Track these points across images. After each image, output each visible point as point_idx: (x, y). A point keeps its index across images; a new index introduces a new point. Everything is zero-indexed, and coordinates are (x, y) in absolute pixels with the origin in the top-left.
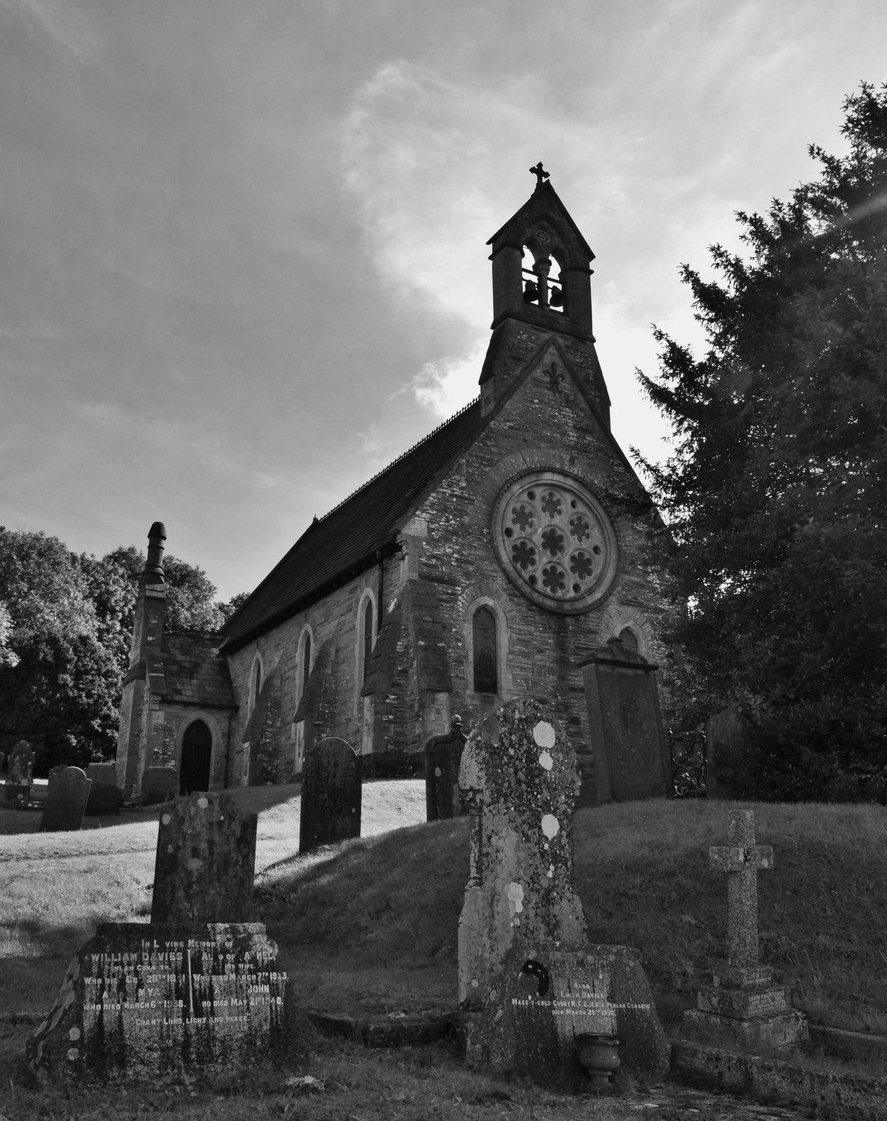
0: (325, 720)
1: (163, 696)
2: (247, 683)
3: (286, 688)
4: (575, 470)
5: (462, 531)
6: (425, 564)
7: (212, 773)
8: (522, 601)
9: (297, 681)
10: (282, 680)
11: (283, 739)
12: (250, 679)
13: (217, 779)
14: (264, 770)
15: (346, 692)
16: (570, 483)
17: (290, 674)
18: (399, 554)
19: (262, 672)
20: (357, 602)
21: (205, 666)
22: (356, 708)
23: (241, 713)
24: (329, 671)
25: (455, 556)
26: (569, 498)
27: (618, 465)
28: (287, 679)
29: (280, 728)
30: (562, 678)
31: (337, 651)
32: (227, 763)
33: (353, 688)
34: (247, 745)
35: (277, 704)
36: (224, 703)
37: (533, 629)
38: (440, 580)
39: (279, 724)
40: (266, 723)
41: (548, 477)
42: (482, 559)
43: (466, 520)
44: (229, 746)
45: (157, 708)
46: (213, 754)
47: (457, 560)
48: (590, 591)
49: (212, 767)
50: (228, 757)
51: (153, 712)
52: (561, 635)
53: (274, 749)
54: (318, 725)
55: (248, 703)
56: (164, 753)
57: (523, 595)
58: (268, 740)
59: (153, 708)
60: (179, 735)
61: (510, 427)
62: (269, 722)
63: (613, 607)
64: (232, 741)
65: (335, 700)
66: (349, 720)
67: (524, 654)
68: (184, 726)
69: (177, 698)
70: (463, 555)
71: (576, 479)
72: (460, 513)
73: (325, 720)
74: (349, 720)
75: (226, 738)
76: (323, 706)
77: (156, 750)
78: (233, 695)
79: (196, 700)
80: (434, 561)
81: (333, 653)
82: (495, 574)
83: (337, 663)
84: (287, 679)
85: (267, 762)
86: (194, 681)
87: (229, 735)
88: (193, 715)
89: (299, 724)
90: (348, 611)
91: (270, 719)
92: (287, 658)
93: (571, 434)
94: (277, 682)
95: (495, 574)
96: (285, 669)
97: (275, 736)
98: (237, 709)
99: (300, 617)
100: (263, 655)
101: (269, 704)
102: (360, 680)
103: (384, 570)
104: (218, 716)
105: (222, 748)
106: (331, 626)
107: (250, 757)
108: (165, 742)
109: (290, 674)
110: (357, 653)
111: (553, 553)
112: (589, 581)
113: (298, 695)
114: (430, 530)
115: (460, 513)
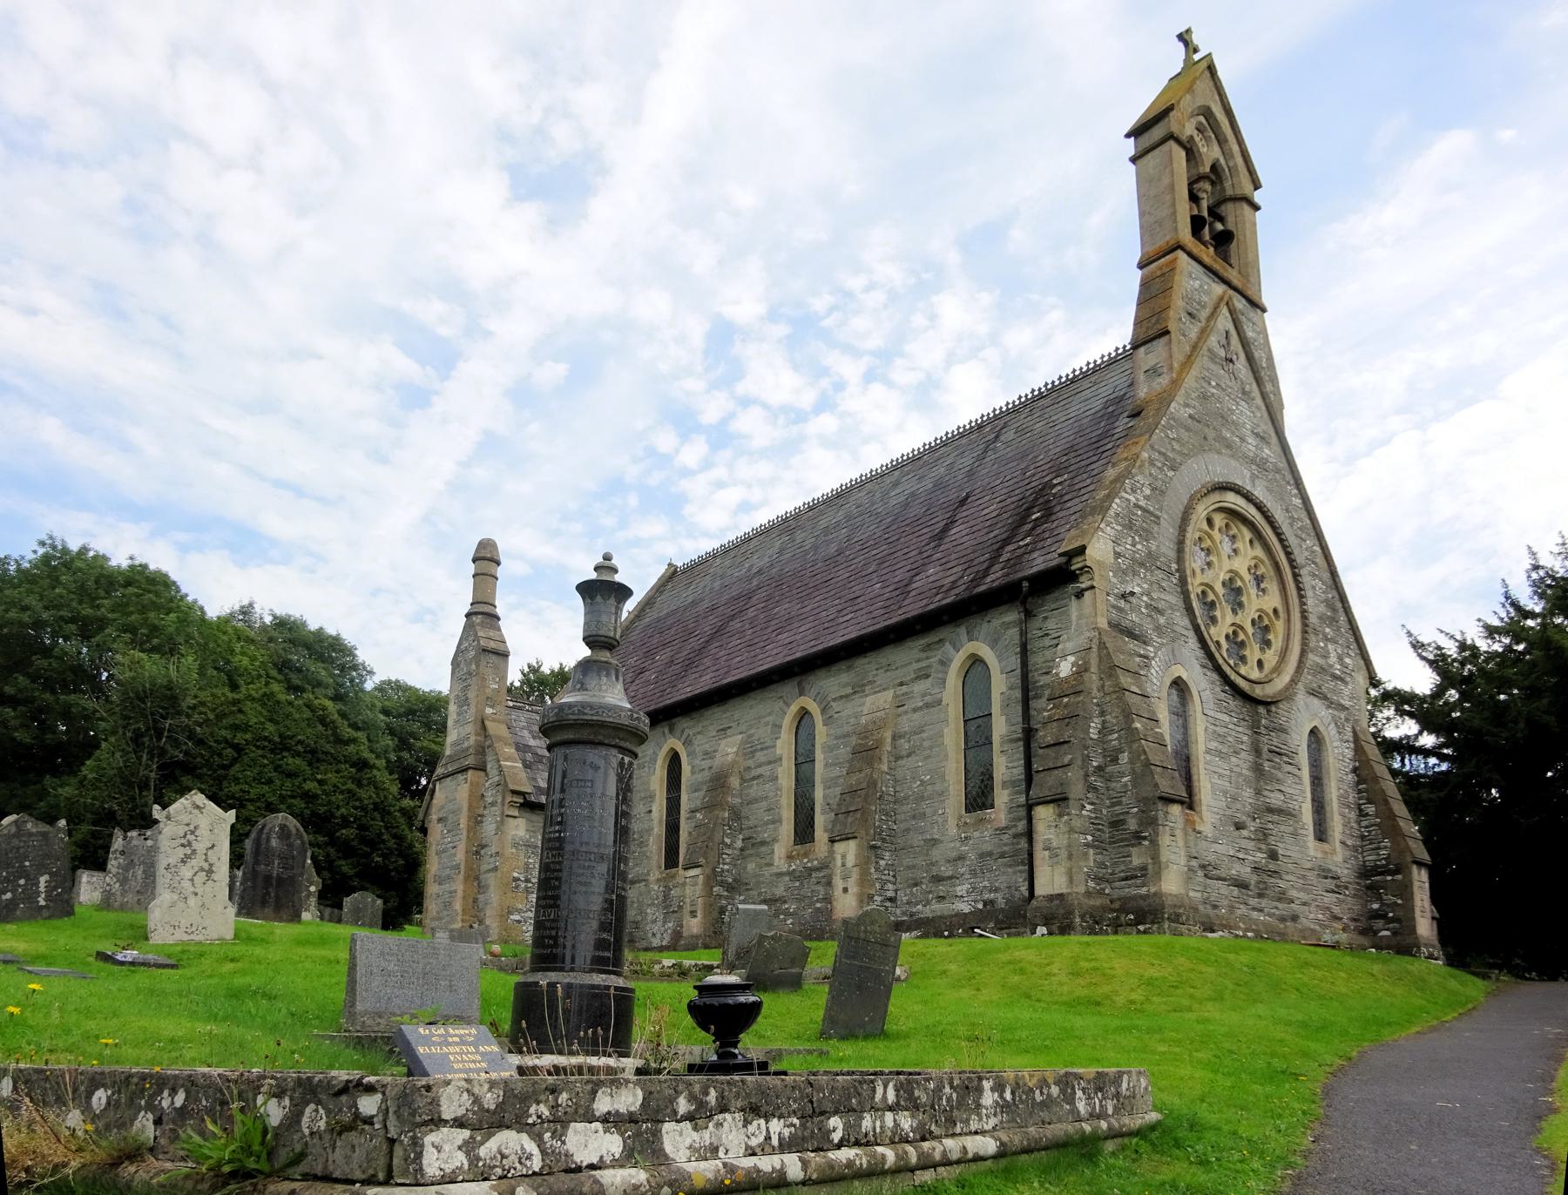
4: (1259, 492)
5: (1149, 561)
6: (1114, 607)
8: (1215, 676)
10: (743, 780)
11: (751, 866)
16: (1252, 512)
18: (1072, 588)
20: (945, 663)
24: (885, 767)
25: (1145, 598)
26: (1248, 535)
27: (1295, 496)
28: (754, 778)
29: (742, 850)
30: (1258, 792)
31: (894, 738)
37: (1226, 718)
38: (1131, 634)
40: (723, 842)
41: (1232, 500)
43: (1153, 546)
45: (516, 813)
47: (1148, 606)
48: (1277, 669)
51: (511, 820)
52: (1255, 727)
53: (735, 880)
54: (874, 847)
56: (527, 881)
57: (1218, 669)
58: (726, 867)
59: (510, 813)
61: (1191, 416)
62: (728, 841)
63: (1301, 697)
66: (934, 842)
67: (1219, 753)
70: (1152, 599)
71: (1260, 507)
72: (1147, 535)
73: (884, 840)
74: (934, 842)
77: (516, 875)
80: (1122, 603)
81: (889, 740)
82: (1185, 633)
84: (754, 778)
85: (727, 898)
89: (840, 847)
90: (918, 678)
91: (727, 835)
93: (1250, 441)
95: (1185, 633)
96: (750, 763)
101: (726, 815)
103: (1029, 614)
108: (527, 864)
111: (1234, 611)
114: (1118, 555)
115: (1147, 535)
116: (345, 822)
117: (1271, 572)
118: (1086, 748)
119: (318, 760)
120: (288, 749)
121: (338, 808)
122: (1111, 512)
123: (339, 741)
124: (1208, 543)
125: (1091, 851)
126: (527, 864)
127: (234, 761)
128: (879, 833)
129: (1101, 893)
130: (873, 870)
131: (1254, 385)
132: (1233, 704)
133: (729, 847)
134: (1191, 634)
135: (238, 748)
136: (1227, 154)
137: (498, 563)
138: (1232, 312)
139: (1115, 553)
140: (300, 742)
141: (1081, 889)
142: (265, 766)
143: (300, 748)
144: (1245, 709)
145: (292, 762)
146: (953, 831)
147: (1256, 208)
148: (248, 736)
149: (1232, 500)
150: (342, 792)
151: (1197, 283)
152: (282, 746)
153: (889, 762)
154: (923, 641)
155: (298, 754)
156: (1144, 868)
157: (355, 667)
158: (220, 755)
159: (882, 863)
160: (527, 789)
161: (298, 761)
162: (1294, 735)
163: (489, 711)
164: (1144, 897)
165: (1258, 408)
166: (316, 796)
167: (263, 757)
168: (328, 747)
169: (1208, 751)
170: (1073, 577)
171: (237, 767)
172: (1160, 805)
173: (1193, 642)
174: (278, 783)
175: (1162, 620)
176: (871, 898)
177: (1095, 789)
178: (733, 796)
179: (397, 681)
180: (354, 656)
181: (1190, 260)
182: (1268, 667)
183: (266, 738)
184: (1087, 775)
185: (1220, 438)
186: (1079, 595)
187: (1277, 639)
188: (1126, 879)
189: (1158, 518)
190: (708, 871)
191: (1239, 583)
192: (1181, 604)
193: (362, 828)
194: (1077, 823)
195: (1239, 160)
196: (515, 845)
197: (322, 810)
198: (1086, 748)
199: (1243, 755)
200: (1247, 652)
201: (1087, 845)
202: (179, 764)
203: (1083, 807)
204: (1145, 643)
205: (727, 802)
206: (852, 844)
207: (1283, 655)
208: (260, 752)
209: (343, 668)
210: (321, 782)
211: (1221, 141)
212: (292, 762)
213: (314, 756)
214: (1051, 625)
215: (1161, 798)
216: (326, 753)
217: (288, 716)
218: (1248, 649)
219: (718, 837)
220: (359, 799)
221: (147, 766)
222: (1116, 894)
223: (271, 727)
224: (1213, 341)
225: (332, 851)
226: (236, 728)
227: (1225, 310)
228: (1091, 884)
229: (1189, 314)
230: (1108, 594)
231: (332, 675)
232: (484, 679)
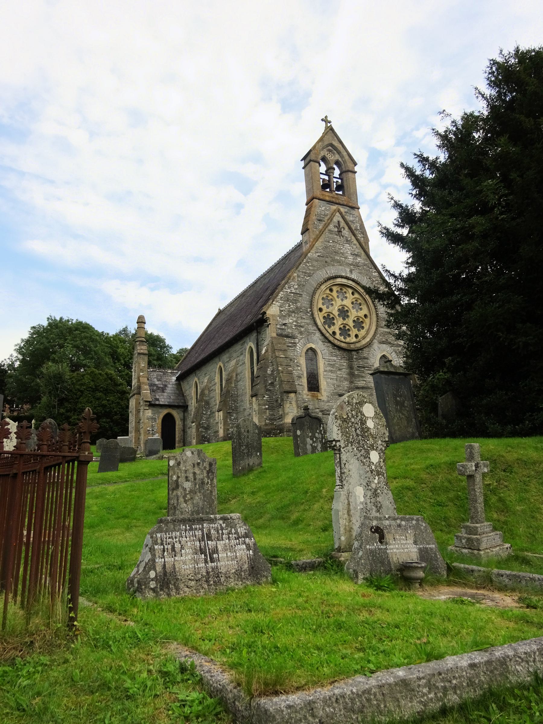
0: (233, 410)
1: (149, 402)
2: (191, 393)
3: (211, 395)
4: (353, 276)
6: (279, 329)
7: (177, 439)
8: (329, 344)
9: (217, 391)
10: (209, 391)
11: (212, 420)
12: (193, 392)
13: (179, 441)
14: (203, 436)
15: (242, 395)
16: (350, 282)
17: (213, 388)
19: (199, 387)
20: (245, 349)
21: (169, 386)
22: (248, 402)
23: (189, 408)
24: (233, 385)
25: (294, 323)
26: (350, 291)
27: (375, 272)
30: (351, 382)
31: (237, 375)
32: (184, 434)
33: (246, 393)
34: (194, 424)
35: (207, 403)
36: (181, 404)
37: (335, 358)
38: (287, 336)
39: (209, 413)
40: (203, 413)
41: (339, 281)
42: (308, 324)
43: (299, 305)
44: (184, 425)
46: (177, 430)
47: (295, 326)
48: (364, 338)
49: (177, 436)
50: (184, 431)
52: (350, 359)
54: (229, 413)
55: (193, 404)
56: (153, 430)
57: (330, 342)
60: (159, 421)
61: (318, 256)
62: (204, 412)
63: (376, 345)
64: (186, 423)
65: (237, 399)
66: (245, 409)
67: (331, 371)
68: (161, 416)
69: (157, 403)
70: (298, 323)
71: (353, 280)
72: (295, 301)
73: (233, 410)
74: (245, 409)
75: (182, 422)
76: (232, 403)
78: (185, 400)
79: (167, 403)
80: (284, 327)
82: (315, 332)
83: (237, 381)
85: (204, 432)
86: (165, 394)
87: (184, 420)
88: (165, 411)
92: (211, 380)
93: (350, 257)
94: (207, 392)
95: (315, 332)
96: (210, 385)
97: (208, 419)
98: (187, 406)
99: (217, 359)
100: (199, 379)
102: (249, 389)
103: (259, 333)
104: (178, 410)
105: (181, 426)
106: (233, 363)
107: (196, 430)
108: (152, 425)
109: (213, 388)
110: (247, 375)
111: (344, 319)
112: (362, 333)
113: (218, 399)
114: (281, 311)
115: (295, 301)
116: (116, 414)
117: (364, 302)
118: (266, 377)
119: (108, 393)
120: (98, 390)
121: (113, 409)
122: (279, 297)
123: (116, 385)
124: (331, 297)
125: (268, 411)
126: (152, 425)
127: (81, 396)
128: (231, 408)
129: (272, 424)
130: (229, 420)
131: (353, 237)
132: (338, 352)
133: (205, 414)
134: (318, 331)
135: (82, 392)
136: (342, 157)
137: (145, 323)
138: (341, 213)
139: (280, 310)
140: (102, 387)
141: (264, 423)
142: (90, 397)
143: (102, 390)
144: (345, 354)
145: (99, 394)
146: (248, 405)
147: (355, 172)
148: (85, 387)
149: (339, 281)
150: (115, 403)
151: (323, 208)
152: (96, 389)
153: (235, 383)
154: (241, 342)
155: (101, 391)
156: (282, 415)
157: (165, 347)
158: (76, 395)
159: (232, 417)
160: (151, 400)
161: (101, 394)
162: (371, 359)
163: (141, 374)
164: (282, 424)
165: (355, 245)
166: (106, 406)
167: (89, 394)
168: (111, 388)
169: (325, 371)
170: (266, 321)
171: (81, 398)
172: (285, 394)
173: (318, 334)
174: (94, 402)
175: (302, 329)
176: (228, 430)
177: (270, 390)
178: (206, 397)
179: (186, 349)
180: (165, 342)
181: (320, 201)
182: (360, 337)
183: (90, 387)
184: (266, 386)
185: (333, 260)
186: (268, 326)
187: (366, 326)
188: (279, 419)
189: (302, 295)
190: (197, 423)
191: (346, 308)
192: (312, 322)
193: (122, 415)
194: (262, 402)
195: (347, 157)
196: (148, 419)
197: (108, 410)
198: (266, 377)
199: (344, 370)
200: (350, 333)
201: (266, 409)
202: (64, 398)
203: (264, 397)
204: (294, 338)
205: (204, 399)
206: (221, 412)
207: (367, 333)
208: (88, 392)
209: (161, 347)
210: (108, 400)
211: (339, 153)
212: (99, 394)
213: (106, 391)
214: (263, 336)
215: (285, 392)
216: (110, 390)
217: (98, 379)
219: (200, 412)
220: (121, 405)
221: (54, 401)
222: (278, 424)
223: (92, 383)
224: (331, 227)
225: (111, 424)
226: (82, 385)
227: (338, 214)
228: (267, 421)
229: (319, 220)
230: (276, 325)
231: (156, 351)
232: (139, 363)
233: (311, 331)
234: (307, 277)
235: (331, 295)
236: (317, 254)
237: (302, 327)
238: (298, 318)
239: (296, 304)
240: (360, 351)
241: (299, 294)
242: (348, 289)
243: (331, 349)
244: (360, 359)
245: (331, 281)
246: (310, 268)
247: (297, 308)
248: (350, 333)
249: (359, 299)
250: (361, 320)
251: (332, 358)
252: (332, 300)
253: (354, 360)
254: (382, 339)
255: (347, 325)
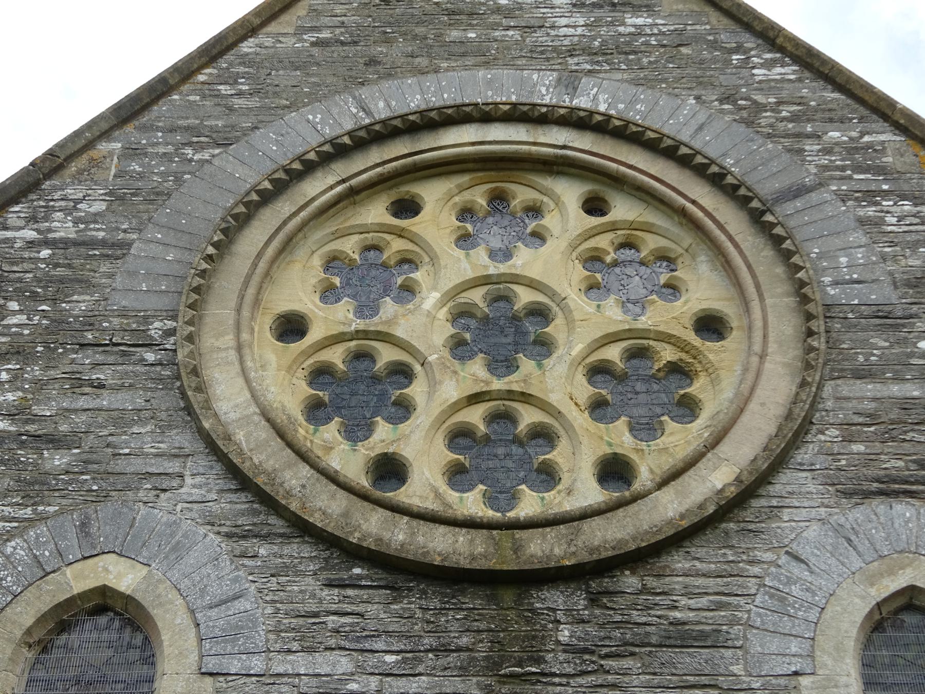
37: (343, 663)
82: (173, 466)
95: (173, 466)
117: (687, 239)
124: (397, 245)
134: (203, 462)
175: (58, 460)
182: (644, 477)
218: (563, 445)
233: (137, 465)
234: (199, 147)
235: (401, 234)
236: (310, 37)
237: (56, 442)
238: (39, 385)
239: (54, 301)
240: (630, 581)
241: (103, 243)
242: (547, 182)
243: (310, 583)
244: (625, 650)
245: (399, 147)
246: (238, 102)
247: (59, 323)
248: (559, 456)
249: (648, 229)
250: (668, 354)
251: (300, 663)
252: (407, 261)
253: (556, 662)
254: (869, 459)
255: (525, 398)
